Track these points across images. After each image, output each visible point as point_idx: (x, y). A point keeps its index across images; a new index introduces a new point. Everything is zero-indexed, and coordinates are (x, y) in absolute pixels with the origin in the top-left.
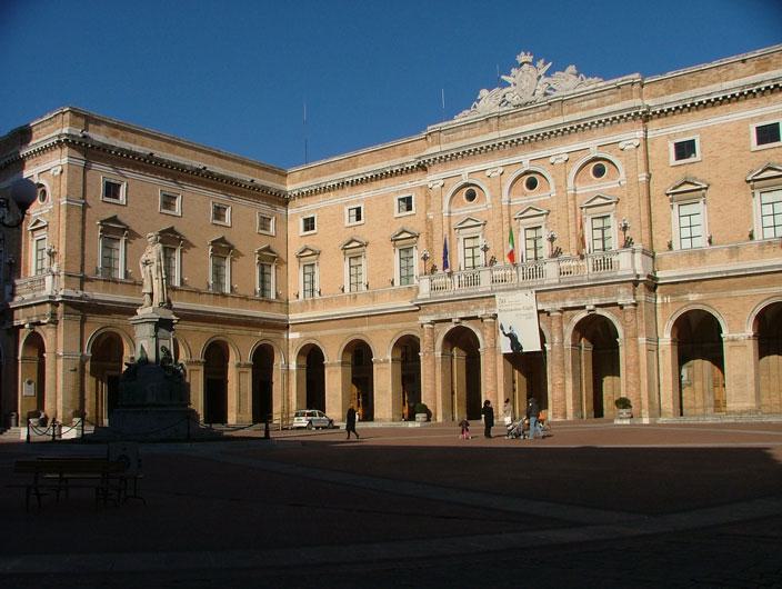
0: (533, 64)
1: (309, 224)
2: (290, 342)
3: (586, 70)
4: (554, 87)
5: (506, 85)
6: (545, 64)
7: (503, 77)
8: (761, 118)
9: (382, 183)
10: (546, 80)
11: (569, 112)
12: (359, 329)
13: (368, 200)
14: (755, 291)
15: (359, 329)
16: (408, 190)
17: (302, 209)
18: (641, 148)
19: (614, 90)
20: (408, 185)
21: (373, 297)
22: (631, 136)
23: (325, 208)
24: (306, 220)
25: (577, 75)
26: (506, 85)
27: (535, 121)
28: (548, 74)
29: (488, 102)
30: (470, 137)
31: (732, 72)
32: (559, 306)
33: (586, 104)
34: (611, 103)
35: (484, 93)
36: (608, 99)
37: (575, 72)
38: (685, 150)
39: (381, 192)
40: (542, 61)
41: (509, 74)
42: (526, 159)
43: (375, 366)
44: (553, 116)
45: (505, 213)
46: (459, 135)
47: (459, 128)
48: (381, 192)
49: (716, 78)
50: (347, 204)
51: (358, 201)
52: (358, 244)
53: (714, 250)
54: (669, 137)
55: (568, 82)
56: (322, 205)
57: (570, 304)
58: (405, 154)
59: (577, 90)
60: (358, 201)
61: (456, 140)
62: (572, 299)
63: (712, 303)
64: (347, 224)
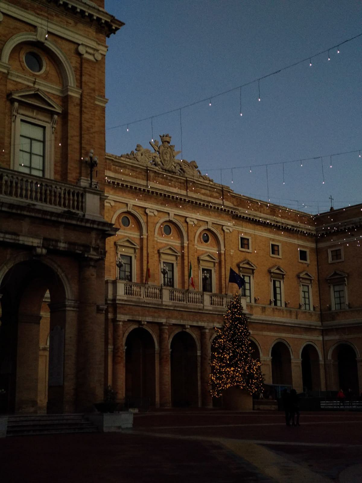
4: (185, 169)
8: (273, 240)
14: (272, 334)
19: (219, 191)
22: (229, 224)
31: (262, 209)
33: (203, 191)
38: (244, 242)
49: (257, 209)
53: (256, 306)
63: (256, 337)
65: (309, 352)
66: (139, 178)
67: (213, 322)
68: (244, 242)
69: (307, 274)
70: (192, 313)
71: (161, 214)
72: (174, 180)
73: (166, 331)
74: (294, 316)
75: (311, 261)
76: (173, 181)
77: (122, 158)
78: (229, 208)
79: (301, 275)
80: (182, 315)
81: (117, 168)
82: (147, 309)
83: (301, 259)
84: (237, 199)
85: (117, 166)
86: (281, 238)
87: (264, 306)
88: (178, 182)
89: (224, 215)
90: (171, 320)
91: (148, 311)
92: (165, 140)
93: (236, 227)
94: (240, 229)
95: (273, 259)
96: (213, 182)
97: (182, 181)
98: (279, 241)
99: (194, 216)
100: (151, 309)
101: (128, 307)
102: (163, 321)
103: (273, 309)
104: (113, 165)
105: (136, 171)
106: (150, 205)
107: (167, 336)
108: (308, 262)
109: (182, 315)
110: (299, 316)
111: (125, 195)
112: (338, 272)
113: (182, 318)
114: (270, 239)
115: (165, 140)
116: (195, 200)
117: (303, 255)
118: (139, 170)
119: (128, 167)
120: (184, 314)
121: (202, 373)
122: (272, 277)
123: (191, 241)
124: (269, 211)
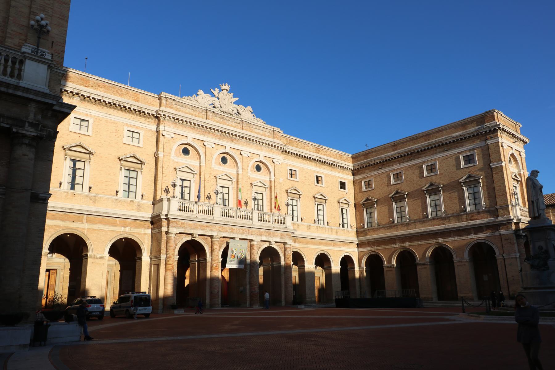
0: (229, 92)
3: (257, 113)
4: (241, 112)
5: (213, 95)
6: (234, 97)
7: (212, 90)
8: (318, 172)
9: (111, 111)
10: (236, 106)
11: (249, 131)
16: (137, 128)
19: (271, 131)
20: (139, 125)
21: (94, 200)
22: (279, 158)
25: (252, 113)
26: (213, 95)
27: (232, 126)
28: (235, 103)
29: (203, 99)
30: (192, 114)
33: (257, 131)
35: (201, 92)
37: (252, 111)
39: (113, 118)
40: (232, 94)
41: (214, 90)
42: (229, 146)
43: (90, 261)
46: (184, 109)
47: (186, 106)
51: (87, 115)
52: (87, 152)
55: (247, 113)
58: (137, 100)
60: (87, 115)
61: (183, 112)
63: (301, 249)
65: (346, 261)
68: (292, 173)
69: (345, 200)
71: (217, 146)
72: (231, 120)
73: (216, 243)
74: (334, 232)
75: (349, 190)
79: (341, 201)
81: (179, 107)
83: (341, 188)
86: (323, 171)
87: (309, 224)
89: (274, 149)
90: (221, 233)
94: (289, 162)
95: (317, 187)
97: (239, 121)
98: (322, 173)
99: (247, 149)
102: (214, 234)
103: (317, 227)
107: (218, 247)
108: (347, 190)
110: (339, 233)
112: (369, 198)
113: (232, 231)
114: (315, 171)
117: (343, 185)
118: (199, 110)
119: (189, 107)
121: (250, 279)
122: (316, 201)
123: (245, 169)
124: (314, 149)
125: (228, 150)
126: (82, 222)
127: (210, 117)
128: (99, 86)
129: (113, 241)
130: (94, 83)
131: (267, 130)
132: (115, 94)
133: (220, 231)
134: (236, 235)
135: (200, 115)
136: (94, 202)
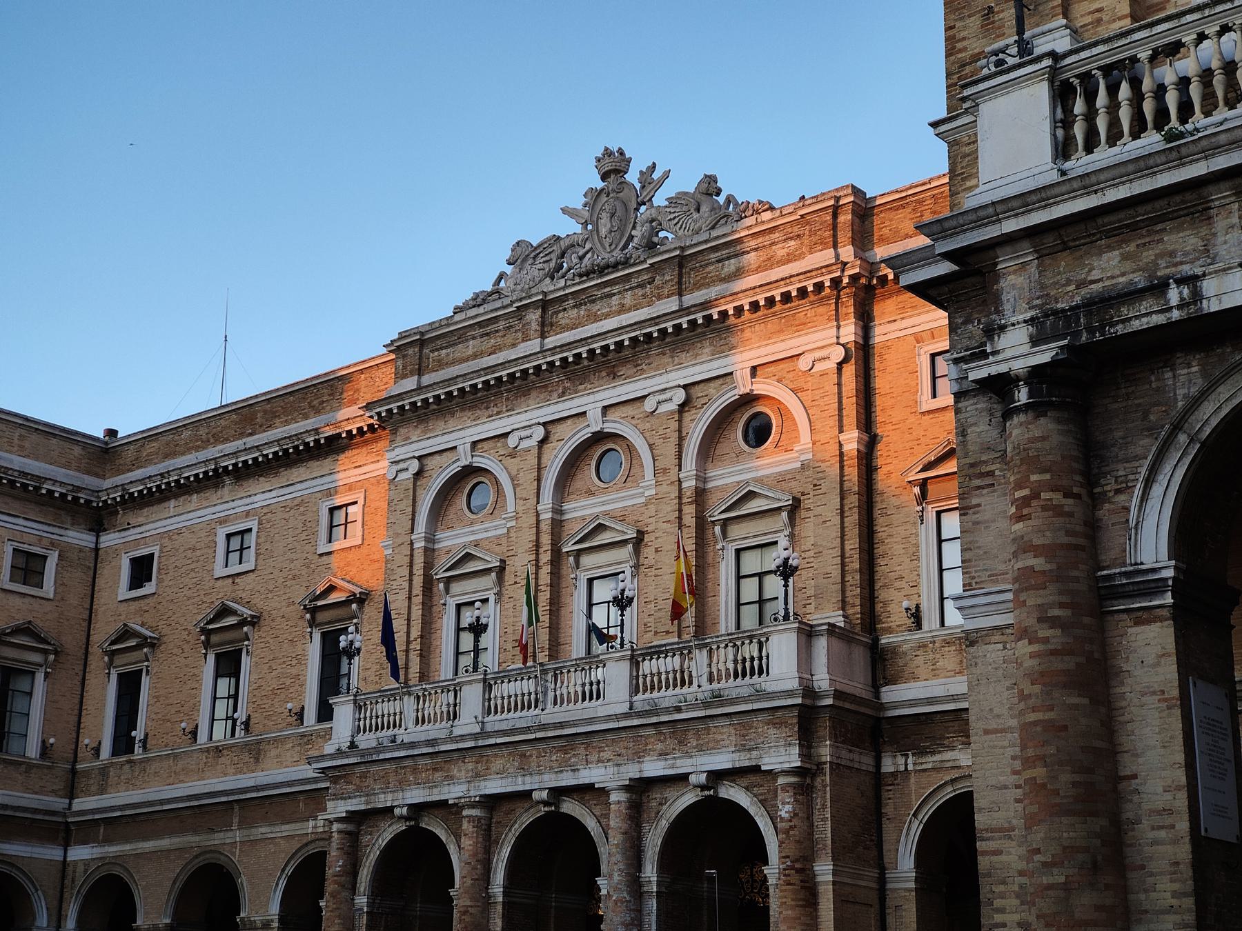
1: (142, 570)
2: (70, 869)
9: (297, 473)
11: (698, 286)
12: (216, 839)
13: (264, 515)
15: (216, 839)
17: (132, 535)
18: (850, 370)
23: (179, 532)
24: (135, 562)
27: (622, 310)
32: (632, 771)
34: (790, 258)
36: (780, 251)
39: (297, 491)
42: (591, 403)
44: (659, 298)
45: (546, 540)
46: (460, 351)
48: (297, 491)
50: (223, 521)
54: (918, 339)
56: (172, 524)
57: (653, 768)
59: (715, 233)
60: (247, 514)
61: (454, 363)
62: (663, 754)
64: (220, 571)
66: (500, 350)
67: (638, 756)
70: (552, 744)
72: (616, 289)
73: (466, 825)
76: (614, 295)
77: (458, 317)
78: (800, 281)
80: (523, 756)
82: (410, 763)
84: (920, 202)
85: (442, 349)
88: (631, 289)
89: (805, 310)
91: (415, 770)
92: (613, 166)
93: (904, 323)
96: (771, 208)
100: (421, 762)
101: (357, 770)
102: (452, 792)
104: (433, 351)
105: (497, 331)
106: (523, 417)
109: (523, 756)
111: (452, 423)
115: (613, 166)
116: (656, 324)
118: (502, 324)
120: (530, 750)
123: (665, 471)
125: (596, 423)
126: (227, 827)
127: (535, 326)
128: (275, 415)
129: (290, 870)
130: (265, 412)
131: (776, 236)
132: (306, 417)
133: (478, 775)
134: (536, 778)
135: (509, 340)
136: (257, 760)
